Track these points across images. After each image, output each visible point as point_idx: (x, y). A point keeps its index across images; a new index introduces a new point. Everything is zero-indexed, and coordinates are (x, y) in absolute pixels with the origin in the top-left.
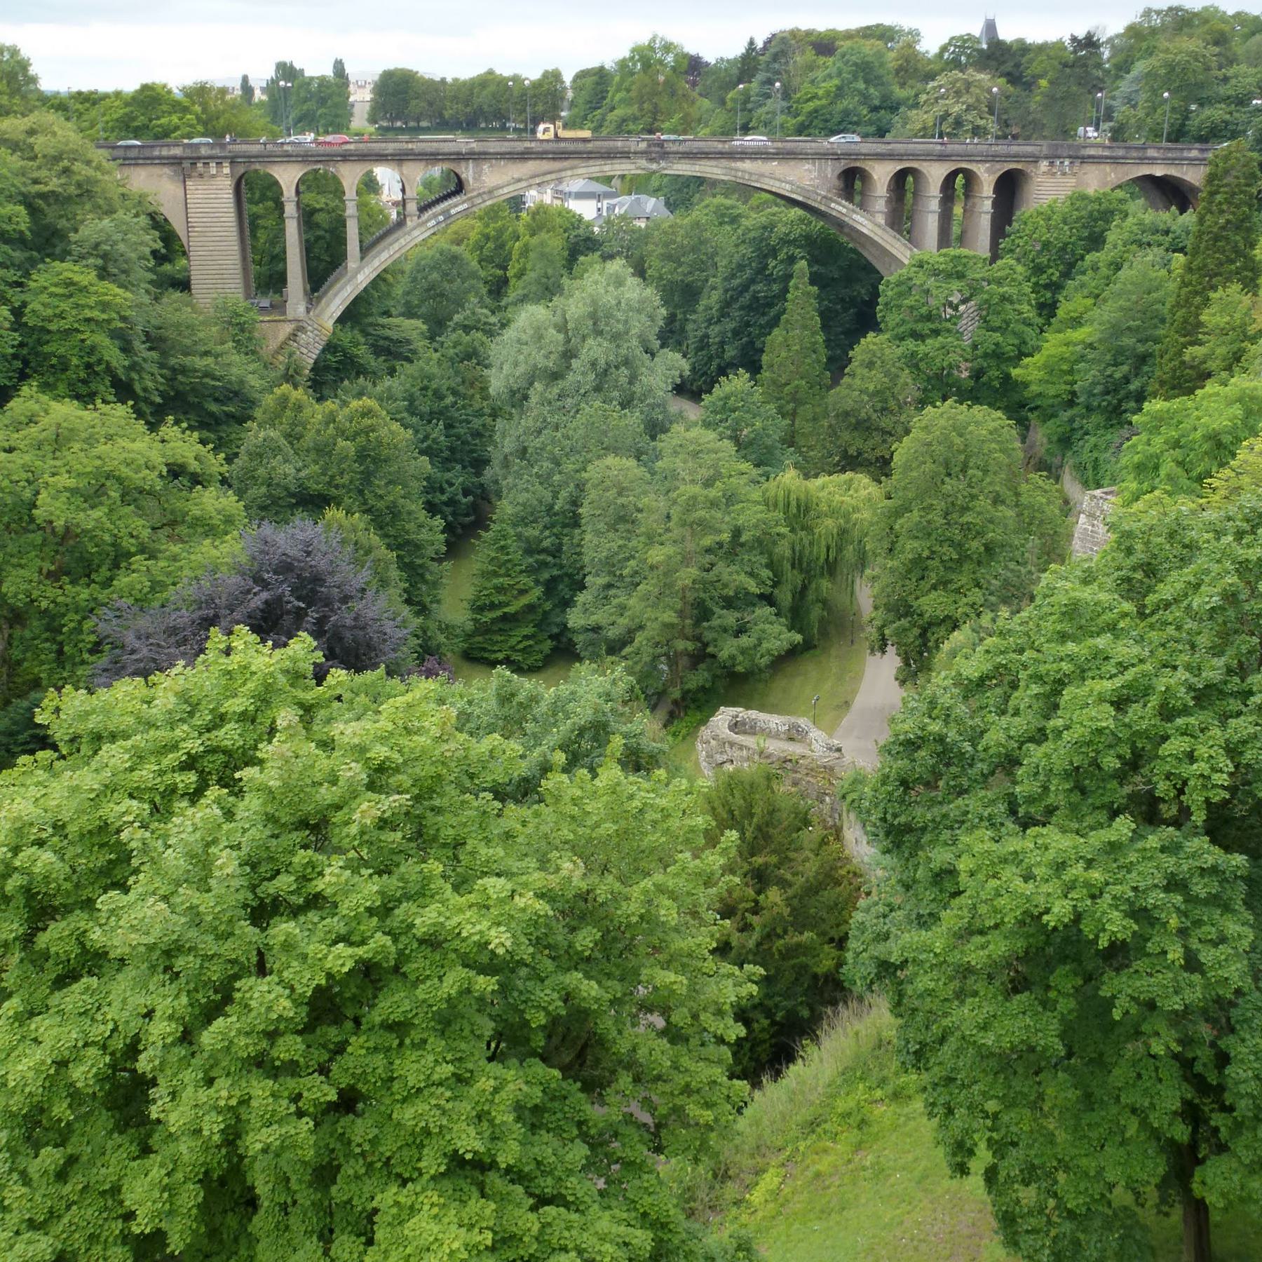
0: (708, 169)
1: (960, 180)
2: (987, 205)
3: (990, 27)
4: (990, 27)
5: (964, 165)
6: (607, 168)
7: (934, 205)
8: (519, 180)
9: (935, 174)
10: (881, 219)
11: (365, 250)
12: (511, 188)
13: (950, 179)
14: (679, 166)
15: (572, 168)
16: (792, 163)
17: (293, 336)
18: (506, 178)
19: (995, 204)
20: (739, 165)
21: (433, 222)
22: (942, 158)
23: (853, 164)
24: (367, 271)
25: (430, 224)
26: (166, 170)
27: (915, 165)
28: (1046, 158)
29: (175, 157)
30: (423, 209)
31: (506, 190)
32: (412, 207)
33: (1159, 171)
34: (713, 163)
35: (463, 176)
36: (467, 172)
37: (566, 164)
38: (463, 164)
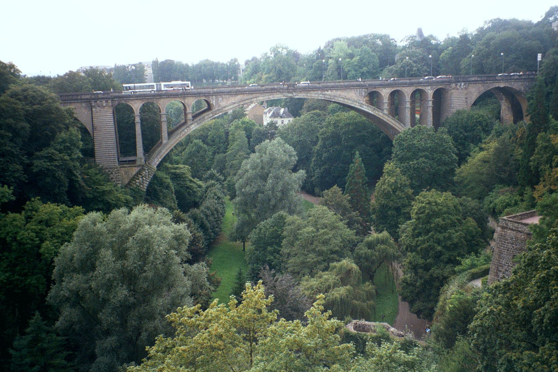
0: (313, 95)
1: (418, 95)
2: (430, 104)
3: (420, 32)
4: (420, 32)
5: (420, 88)
6: (271, 97)
7: (408, 105)
8: (234, 103)
9: (408, 91)
10: (386, 112)
11: (170, 134)
13: (413, 94)
15: (256, 97)
17: (139, 173)
19: (434, 103)
20: (326, 92)
22: (411, 84)
26: (84, 105)
27: (399, 89)
28: (454, 82)
29: (87, 99)
30: (194, 117)
32: (190, 116)
33: (502, 85)
34: (315, 92)
36: (213, 101)
37: (254, 95)
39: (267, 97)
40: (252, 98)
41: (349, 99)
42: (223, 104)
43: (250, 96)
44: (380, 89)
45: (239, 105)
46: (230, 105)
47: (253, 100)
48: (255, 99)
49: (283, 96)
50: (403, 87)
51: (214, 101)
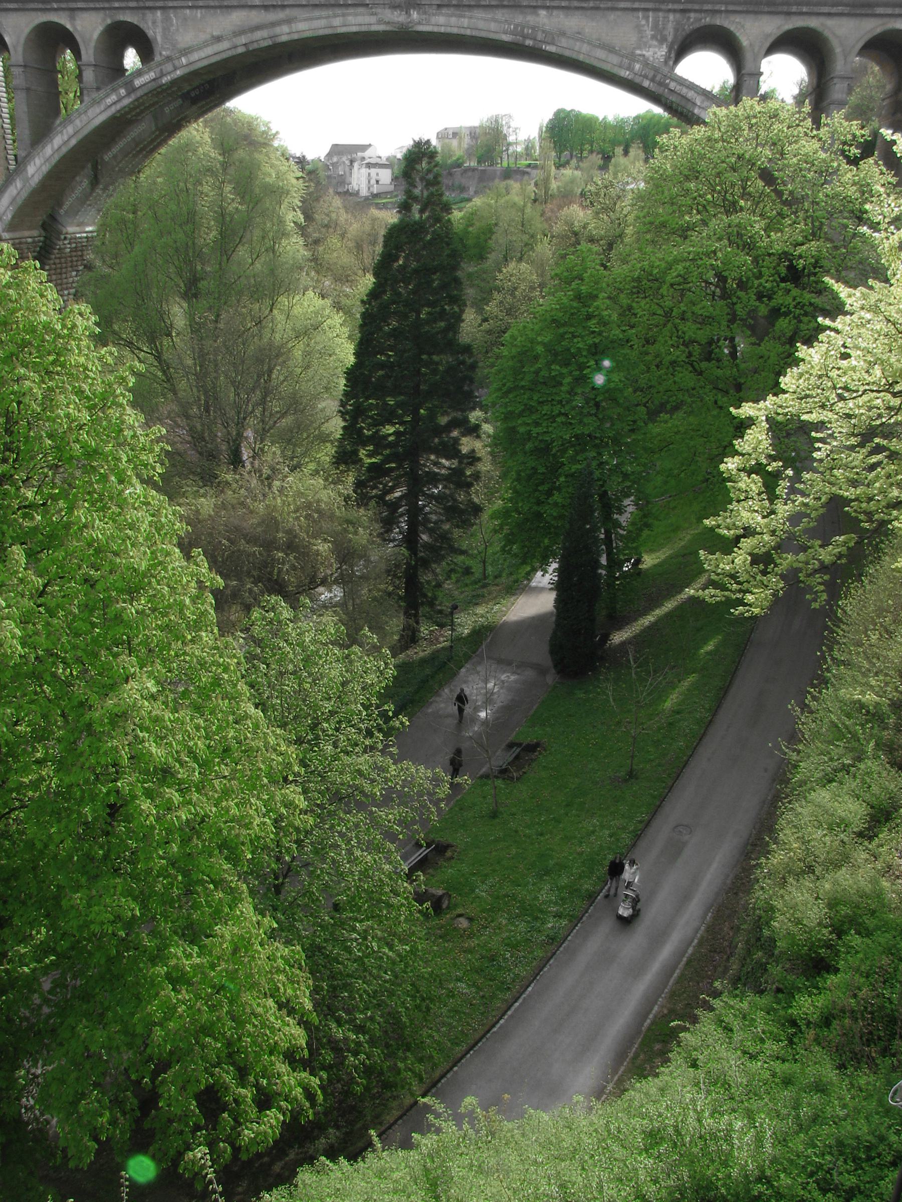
0: (481, 24)
6: (337, 22)
8: (218, 39)
12: (209, 51)
14: (441, 20)
15: (289, 21)
16: (612, 16)
18: (203, 37)
21: (114, 97)
23: (708, 20)
24: (38, 161)
25: (109, 101)
31: (202, 54)
35: (150, 33)
37: (281, 15)
38: (149, 15)
39: (323, 23)
40: (273, 24)
41: (611, 49)
42: (186, 38)
43: (272, 16)
44: (738, 18)
45: (236, 47)
46: (206, 44)
47: (277, 30)
48: (285, 29)
49: (380, 22)
50: (829, 15)
51: (159, 30)
